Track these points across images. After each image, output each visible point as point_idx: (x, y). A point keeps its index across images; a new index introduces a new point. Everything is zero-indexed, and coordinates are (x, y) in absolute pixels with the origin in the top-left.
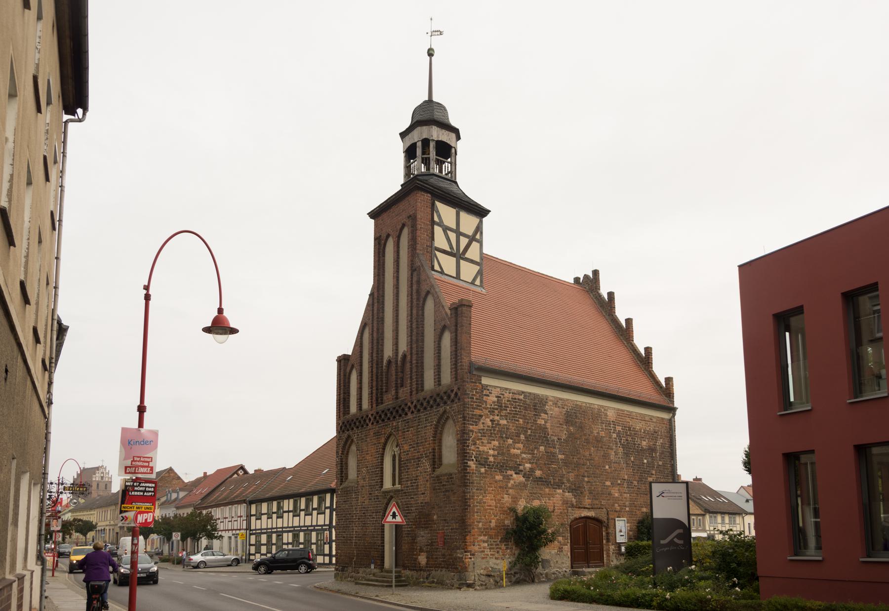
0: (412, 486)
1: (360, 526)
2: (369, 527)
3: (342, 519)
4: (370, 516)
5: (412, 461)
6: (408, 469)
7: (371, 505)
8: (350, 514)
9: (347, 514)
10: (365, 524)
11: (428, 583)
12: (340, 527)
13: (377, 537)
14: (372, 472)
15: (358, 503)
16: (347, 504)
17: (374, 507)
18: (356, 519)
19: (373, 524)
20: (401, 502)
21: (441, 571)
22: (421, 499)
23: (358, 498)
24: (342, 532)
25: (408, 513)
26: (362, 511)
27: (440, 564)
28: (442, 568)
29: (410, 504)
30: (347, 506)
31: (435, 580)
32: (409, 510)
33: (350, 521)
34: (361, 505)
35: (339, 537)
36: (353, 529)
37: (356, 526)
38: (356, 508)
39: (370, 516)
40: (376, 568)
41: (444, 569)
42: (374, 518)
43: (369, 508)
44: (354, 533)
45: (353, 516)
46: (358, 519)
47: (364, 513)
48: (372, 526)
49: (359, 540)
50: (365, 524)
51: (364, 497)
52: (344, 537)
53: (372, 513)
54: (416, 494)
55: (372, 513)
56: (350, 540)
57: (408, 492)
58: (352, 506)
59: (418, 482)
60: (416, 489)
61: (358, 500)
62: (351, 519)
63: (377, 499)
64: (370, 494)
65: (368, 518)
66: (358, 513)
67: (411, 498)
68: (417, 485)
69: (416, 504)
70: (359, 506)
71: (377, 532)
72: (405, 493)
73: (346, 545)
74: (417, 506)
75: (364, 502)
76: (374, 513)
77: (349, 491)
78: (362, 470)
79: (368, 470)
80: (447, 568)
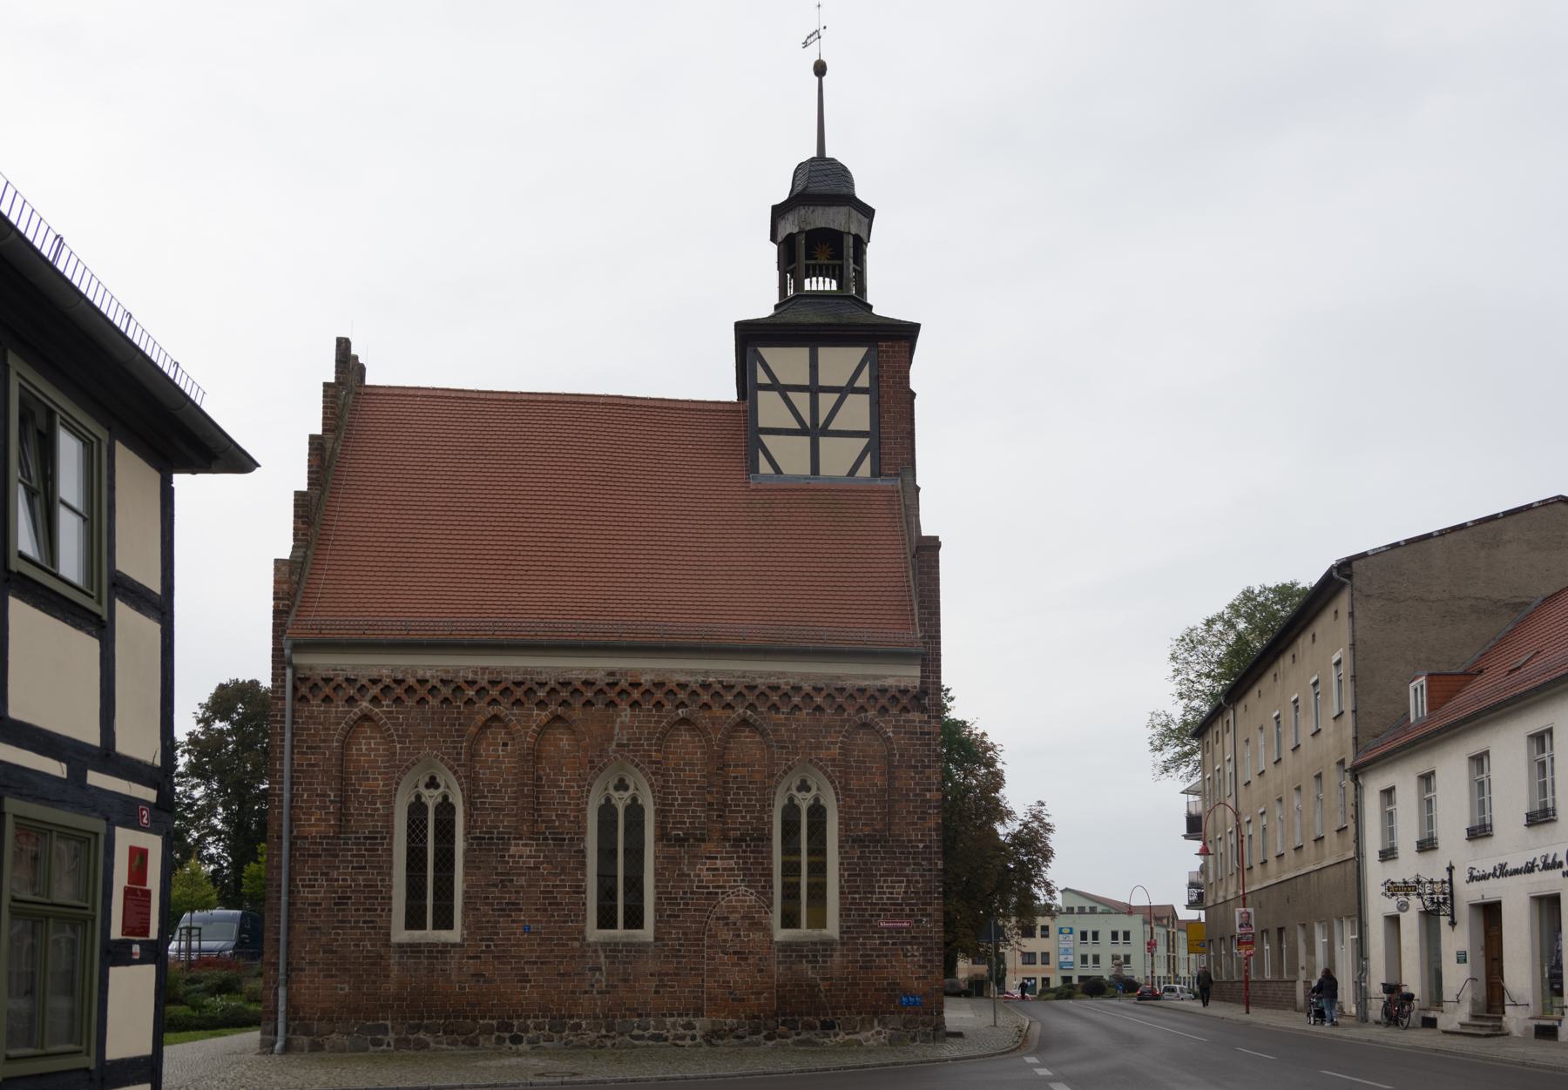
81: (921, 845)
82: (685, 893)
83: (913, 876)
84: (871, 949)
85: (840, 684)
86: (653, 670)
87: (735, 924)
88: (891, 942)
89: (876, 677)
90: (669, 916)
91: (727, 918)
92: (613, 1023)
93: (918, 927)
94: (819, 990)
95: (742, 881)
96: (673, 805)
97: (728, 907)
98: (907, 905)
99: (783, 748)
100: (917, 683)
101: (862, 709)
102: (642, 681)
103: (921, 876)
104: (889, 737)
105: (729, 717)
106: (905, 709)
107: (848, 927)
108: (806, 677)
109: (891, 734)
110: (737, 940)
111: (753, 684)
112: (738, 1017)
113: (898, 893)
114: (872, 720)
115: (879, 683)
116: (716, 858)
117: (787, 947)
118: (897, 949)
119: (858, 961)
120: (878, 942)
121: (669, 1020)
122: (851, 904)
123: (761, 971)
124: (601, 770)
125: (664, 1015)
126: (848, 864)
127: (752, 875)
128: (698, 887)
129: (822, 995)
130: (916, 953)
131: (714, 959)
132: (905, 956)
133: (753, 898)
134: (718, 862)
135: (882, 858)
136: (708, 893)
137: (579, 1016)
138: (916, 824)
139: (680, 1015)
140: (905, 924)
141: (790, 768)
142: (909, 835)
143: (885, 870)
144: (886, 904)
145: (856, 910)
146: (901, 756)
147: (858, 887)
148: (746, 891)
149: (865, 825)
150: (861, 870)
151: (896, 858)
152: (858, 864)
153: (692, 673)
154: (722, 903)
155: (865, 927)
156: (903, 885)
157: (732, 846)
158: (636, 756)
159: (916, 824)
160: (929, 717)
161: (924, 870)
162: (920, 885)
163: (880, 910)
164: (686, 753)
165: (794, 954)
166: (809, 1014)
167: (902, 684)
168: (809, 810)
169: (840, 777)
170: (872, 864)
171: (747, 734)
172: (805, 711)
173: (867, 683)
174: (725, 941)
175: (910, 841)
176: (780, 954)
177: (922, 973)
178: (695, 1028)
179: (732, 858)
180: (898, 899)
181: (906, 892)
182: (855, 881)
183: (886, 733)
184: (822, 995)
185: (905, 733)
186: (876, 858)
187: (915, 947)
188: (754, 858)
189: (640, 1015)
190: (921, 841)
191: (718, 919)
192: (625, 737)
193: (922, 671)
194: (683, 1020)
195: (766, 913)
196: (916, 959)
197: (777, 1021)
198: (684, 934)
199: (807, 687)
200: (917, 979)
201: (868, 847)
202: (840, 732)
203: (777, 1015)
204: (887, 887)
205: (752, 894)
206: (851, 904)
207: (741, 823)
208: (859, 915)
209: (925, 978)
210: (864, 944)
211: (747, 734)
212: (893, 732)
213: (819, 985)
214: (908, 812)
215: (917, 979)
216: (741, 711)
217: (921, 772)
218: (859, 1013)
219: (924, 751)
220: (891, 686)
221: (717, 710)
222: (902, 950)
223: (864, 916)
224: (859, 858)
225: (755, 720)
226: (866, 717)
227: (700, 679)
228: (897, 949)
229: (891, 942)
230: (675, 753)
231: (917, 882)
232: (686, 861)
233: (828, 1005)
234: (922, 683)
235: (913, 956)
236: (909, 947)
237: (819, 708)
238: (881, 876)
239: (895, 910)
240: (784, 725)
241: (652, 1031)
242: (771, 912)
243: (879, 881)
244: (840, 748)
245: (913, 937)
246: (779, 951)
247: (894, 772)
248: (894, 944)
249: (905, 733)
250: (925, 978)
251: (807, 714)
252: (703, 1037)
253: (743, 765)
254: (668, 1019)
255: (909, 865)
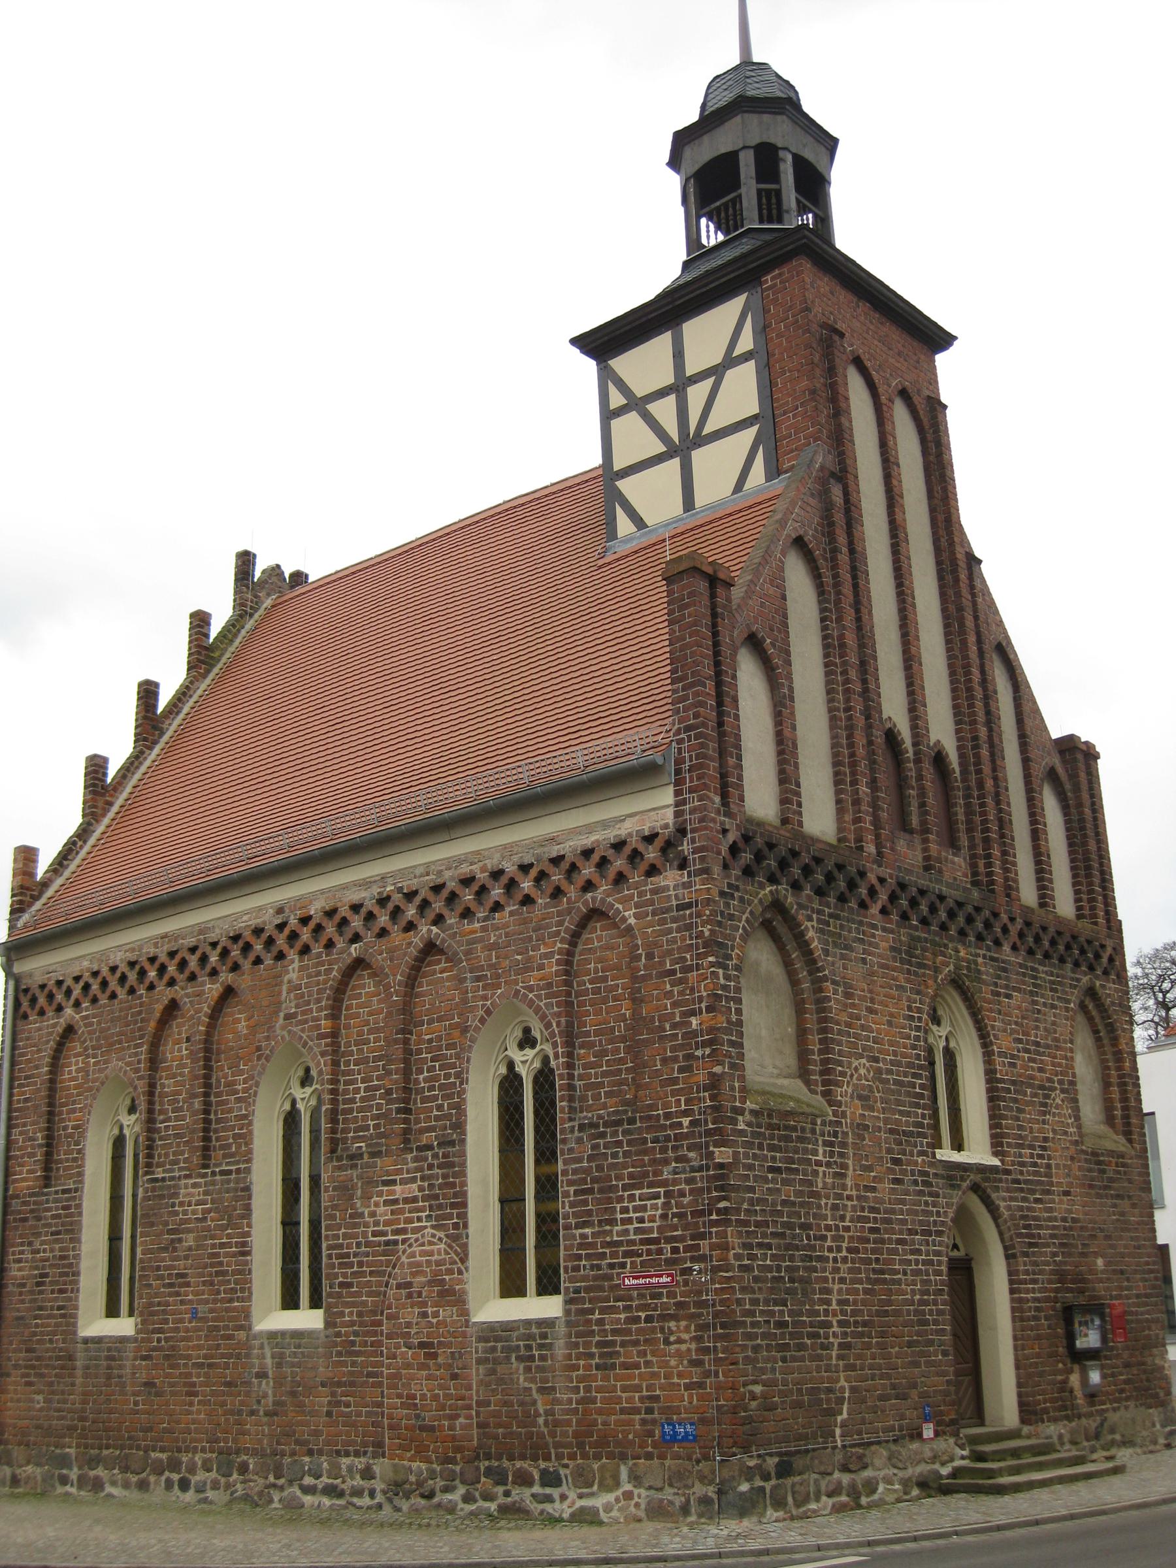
0: (1035, 1165)
1: (860, 1282)
2: (899, 1282)
3: (769, 1247)
4: (900, 1242)
5: (1029, 1091)
6: (1020, 1110)
7: (903, 1202)
8: (804, 1227)
9: (789, 1226)
10: (882, 1272)
11: (1103, 1449)
12: (756, 1279)
13: (936, 1322)
14: (896, 1082)
15: (844, 1187)
16: (786, 1182)
17: (916, 1213)
18: (839, 1249)
19: (917, 1273)
20: (1009, 1208)
21: (1126, 1408)
22: (1061, 1206)
23: (844, 1166)
24: (767, 1302)
25: (1031, 1245)
26: (866, 1220)
27: (1122, 1391)
28: (1127, 1399)
29: (1035, 1219)
30: (788, 1193)
31: (1118, 1437)
32: (1032, 1236)
33: (810, 1258)
34: (859, 1198)
35: (754, 1324)
36: (828, 1291)
37: (842, 1280)
38: (835, 1207)
39: (900, 1242)
40: (944, 1433)
41: (1131, 1404)
42: (919, 1252)
43: (893, 1211)
44: (834, 1306)
45: (824, 1238)
46: (849, 1250)
47: (872, 1230)
48: (914, 1283)
49: (861, 1335)
50: (882, 1272)
51: (869, 1168)
52: (781, 1324)
53: (911, 1232)
54: (1048, 1192)
55: (911, 1232)
56: (815, 1336)
57: (1026, 1182)
58: (816, 1195)
59: (1050, 1158)
60: (1046, 1176)
61: (844, 1176)
62: (813, 1248)
63: (925, 1183)
64: (896, 1162)
65: (895, 1252)
66: (847, 1229)
67: (1037, 1201)
68: (1049, 1166)
69: (1050, 1219)
70: (849, 1198)
71: (935, 1303)
72: (1018, 1182)
73: (794, 1359)
74: (1054, 1228)
75: (874, 1189)
76: (917, 1234)
77: (794, 1129)
78: (855, 1063)
79: (879, 1071)
80: (1137, 1400)
81: (686, 1121)
82: (358, 1245)
83: (675, 1182)
84: (615, 1332)
85: (555, 851)
86: (322, 892)
87: (420, 1294)
88: (643, 1315)
89: (605, 824)
90: (341, 1285)
91: (409, 1285)
92: (281, 1464)
93: (686, 1283)
94: (536, 1411)
95: (429, 1217)
96: (353, 1101)
97: (410, 1265)
98: (669, 1240)
99: (478, 979)
100: (669, 816)
101: (589, 886)
102: (312, 913)
103: (689, 1181)
104: (630, 928)
105: (410, 944)
106: (652, 871)
107: (577, 1291)
108: (507, 850)
109: (632, 921)
110: (423, 1321)
111: (440, 881)
112: (428, 1461)
113: (652, 1219)
114: (603, 901)
115: (612, 835)
116: (393, 1182)
117: (496, 1333)
118: (653, 1330)
119: (592, 1356)
120: (622, 1316)
121: (345, 1461)
122: (581, 1246)
123: (454, 1377)
124: (268, 1059)
125: (338, 1453)
126: (575, 1172)
127: (440, 1207)
128: (375, 1234)
129: (541, 1420)
130: (685, 1336)
131: (395, 1358)
132: (667, 1342)
133: (442, 1246)
134: (398, 1188)
135: (626, 1154)
136: (387, 1243)
137: (246, 1451)
138: (675, 1081)
139: (357, 1454)
140: (664, 1279)
141: (488, 1012)
142: (666, 1105)
143: (631, 1176)
144: (633, 1242)
145: (588, 1257)
146: (650, 956)
147: (589, 1213)
148: (433, 1236)
149: (609, 1094)
150: (594, 1180)
151: (645, 1152)
152: (587, 1171)
153: (365, 884)
154: (404, 1259)
155: (601, 1289)
156: (660, 1202)
157: (416, 1160)
158: (303, 1030)
159: (675, 1081)
160: (689, 876)
161: (693, 1170)
162: (686, 1200)
163: (627, 1254)
164: (370, 1014)
165: (499, 1345)
166: (523, 1457)
167: (646, 828)
168: (536, 1080)
169: (558, 1015)
170: (613, 1166)
171: (443, 965)
172: (508, 909)
173: (593, 838)
174: (409, 1325)
175: (668, 1116)
176: (481, 1345)
177: (696, 1376)
178: (373, 1478)
179: (414, 1180)
180: (651, 1230)
181: (664, 1216)
182: (585, 1203)
183: (624, 919)
184: (541, 1420)
185: (654, 914)
186: (615, 1155)
187: (683, 1323)
188: (445, 1176)
189: (310, 1453)
190: (685, 1113)
191: (399, 1286)
192: (293, 1004)
193: (677, 793)
194: (360, 1463)
195: (460, 1272)
196: (684, 1347)
197: (478, 1468)
198: (360, 1314)
199: (510, 868)
200: (688, 1387)
201: (602, 1135)
202: (558, 933)
203: (477, 1458)
204: (636, 1209)
205: (440, 1239)
206: (581, 1246)
207: (437, 1118)
208: (592, 1267)
209: (701, 1385)
210: (600, 1322)
211: (443, 965)
212: (636, 916)
213: (534, 1402)
214: (664, 1061)
215: (688, 1387)
216: (425, 929)
217: (681, 981)
218: (597, 1457)
219: (683, 939)
220: (630, 835)
221: (397, 936)
222: (662, 1329)
223: (599, 1267)
224: (591, 1158)
225: (444, 940)
226: (594, 899)
227: (375, 890)
228: (653, 1330)
229: (643, 1315)
230: (357, 1015)
231: (682, 1194)
232: (359, 1192)
233: (549, 1440)
234: (677, 814)
235: (680, 1341)
236: (672, 1324)
237: (528, 900)
238: (625, 1188)
239: (649, 1252)
240: (481, 940)
241: (325, 1480)
242: (467, 1269)
243: (620, 1199)
244: (558, 963)
245: (679, 1305)
246: (480, 1339)
247: (639, 990)
248: (649, 1319)
249: (654, 914)
250: (701, 1385)
251: (511, 913)
252: (384, 1492)
253: (440, 1020)
254: (344, 1460)
255: (666, 1162)
